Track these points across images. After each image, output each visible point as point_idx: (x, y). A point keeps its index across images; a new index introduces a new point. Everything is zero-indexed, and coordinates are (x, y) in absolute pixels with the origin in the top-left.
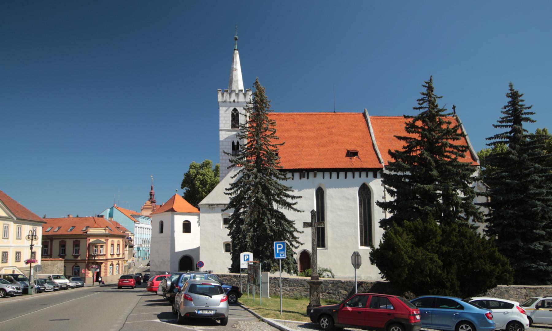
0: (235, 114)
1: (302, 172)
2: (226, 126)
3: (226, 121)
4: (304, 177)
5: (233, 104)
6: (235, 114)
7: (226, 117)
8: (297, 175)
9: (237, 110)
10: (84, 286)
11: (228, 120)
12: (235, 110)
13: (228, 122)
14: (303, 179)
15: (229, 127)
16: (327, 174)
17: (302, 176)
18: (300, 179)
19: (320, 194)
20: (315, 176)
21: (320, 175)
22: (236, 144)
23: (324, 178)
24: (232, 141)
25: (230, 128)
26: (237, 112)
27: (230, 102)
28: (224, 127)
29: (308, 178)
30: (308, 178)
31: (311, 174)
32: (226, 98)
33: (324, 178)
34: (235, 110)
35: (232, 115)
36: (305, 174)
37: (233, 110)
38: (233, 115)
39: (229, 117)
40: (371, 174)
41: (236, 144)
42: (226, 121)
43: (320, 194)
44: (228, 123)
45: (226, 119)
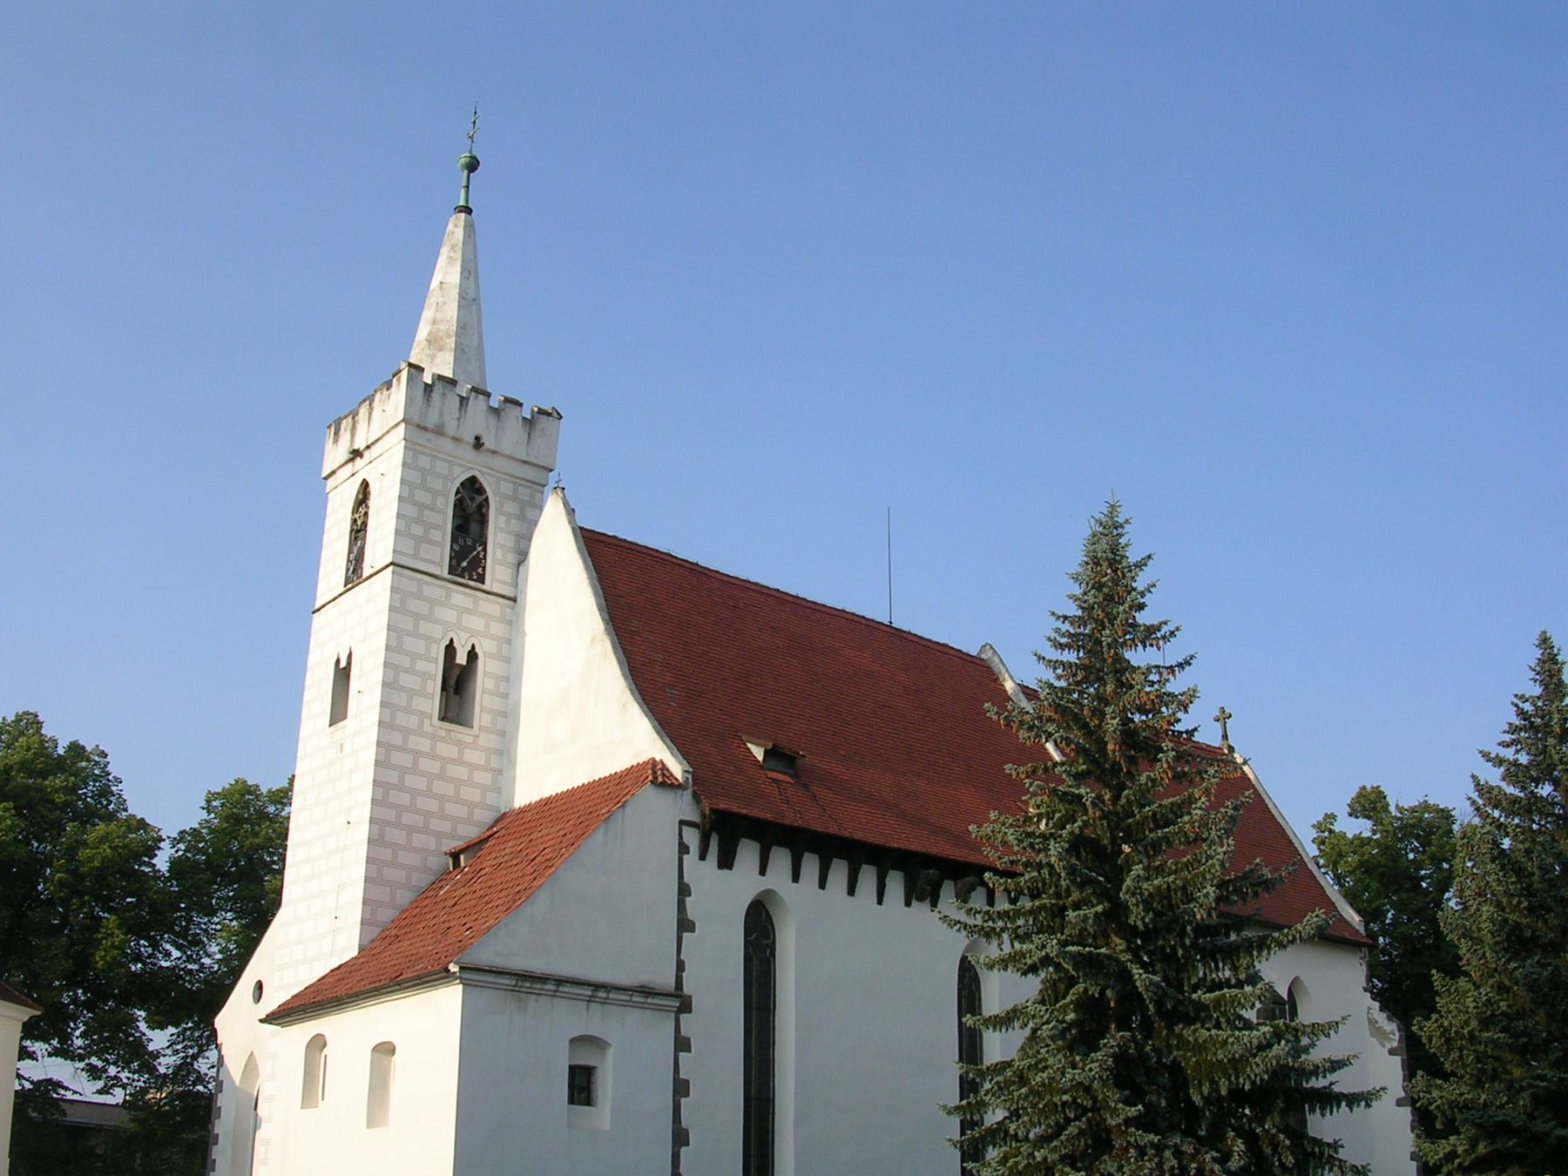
0: (472, 507)
3: (428, 526)
5: (469, 454)
11: (438, 527)
12: (472, 487)
13: (436, 535)
22: (461, 659)
25: (445, 574)
26: (480, 499)
27: (456, 439)
28: (416, 556)
32: (441, 414)
34: (472, 487)
38: (459, 505)
41: (461, 659)
42: (428, 526)
44: (432, 543)
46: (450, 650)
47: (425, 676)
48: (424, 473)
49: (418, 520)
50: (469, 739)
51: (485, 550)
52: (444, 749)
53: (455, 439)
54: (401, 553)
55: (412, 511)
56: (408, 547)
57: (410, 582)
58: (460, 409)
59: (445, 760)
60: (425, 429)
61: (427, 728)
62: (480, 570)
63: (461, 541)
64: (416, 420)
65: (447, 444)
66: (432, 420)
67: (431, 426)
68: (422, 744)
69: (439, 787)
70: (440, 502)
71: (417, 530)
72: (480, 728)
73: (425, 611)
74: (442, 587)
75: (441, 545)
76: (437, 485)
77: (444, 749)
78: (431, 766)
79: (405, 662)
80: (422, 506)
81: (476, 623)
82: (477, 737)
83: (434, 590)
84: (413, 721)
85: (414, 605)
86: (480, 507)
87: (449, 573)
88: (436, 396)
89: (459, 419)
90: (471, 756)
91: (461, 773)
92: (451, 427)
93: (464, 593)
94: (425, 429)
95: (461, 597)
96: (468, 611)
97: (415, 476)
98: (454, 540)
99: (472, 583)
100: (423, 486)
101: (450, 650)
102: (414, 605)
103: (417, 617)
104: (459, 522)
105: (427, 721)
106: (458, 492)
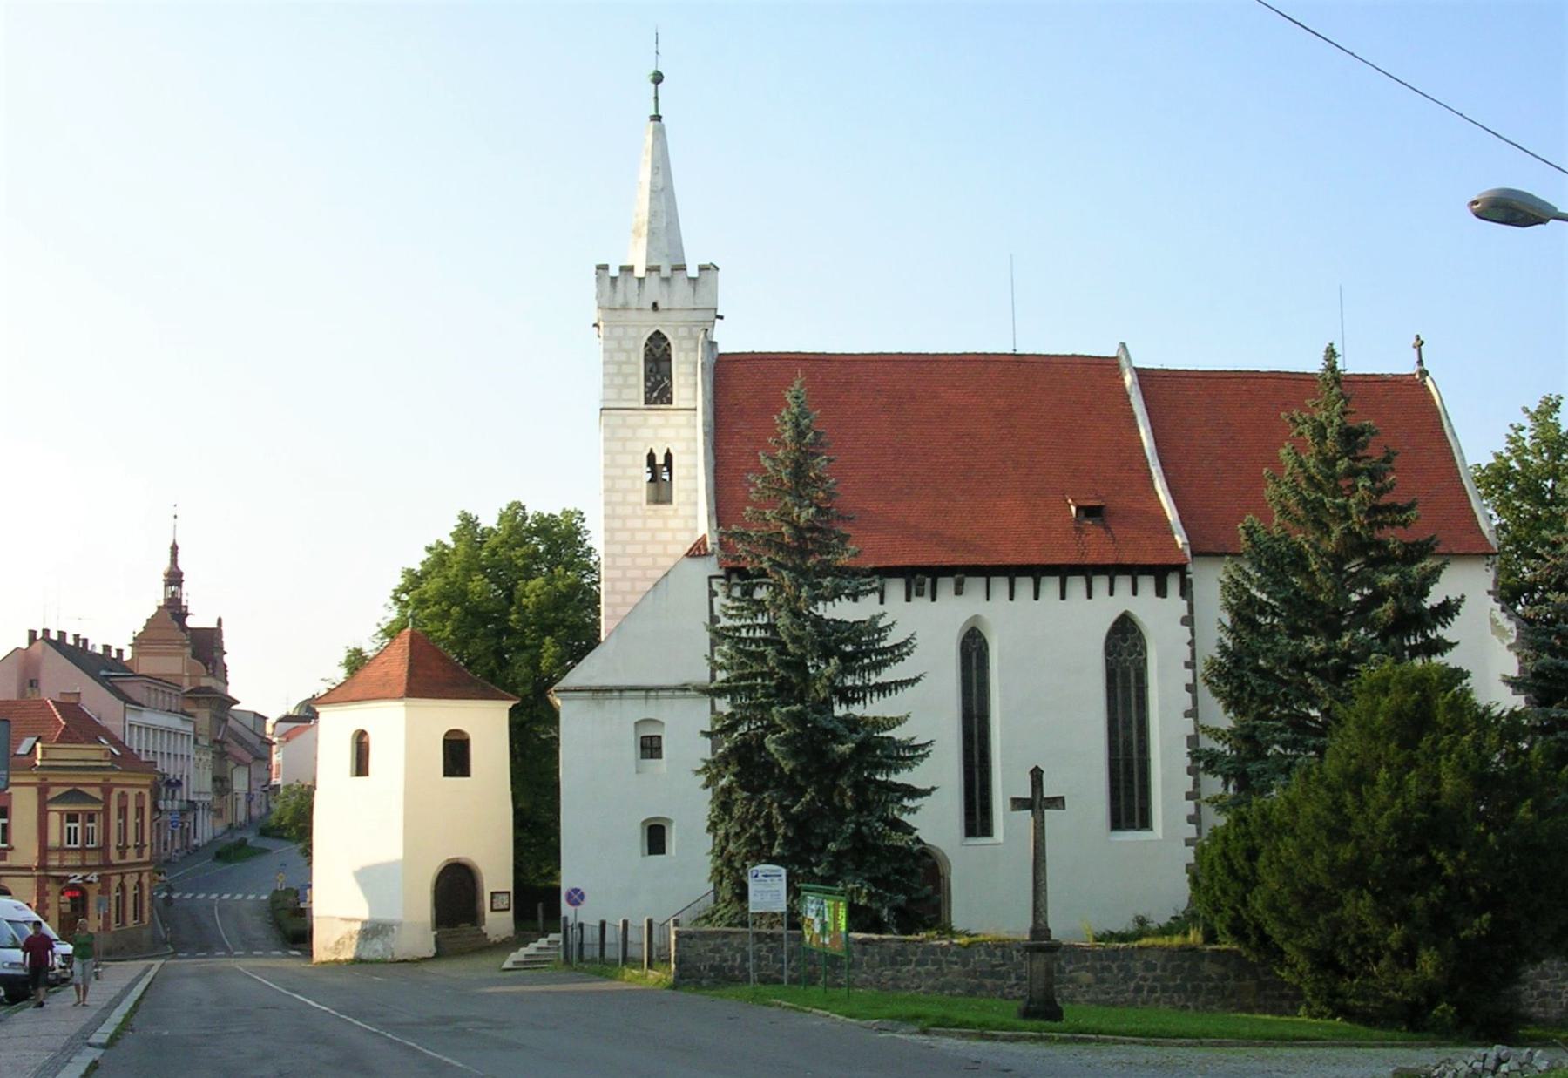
0: (658, 352)
1: (914, 576)
2: (624, 397)
3: (626, 376)
4: (920, 594)
6: (658, 352)
7: (628, 362)
8: (896, 588)
9: (665, 339)
10: (639, 941)
13: (632, 380)
14: (916, 600)
15: (638, 400)
16: (1000, 585)
17: (913, 590)
18: (908, 600)
19: (974, 654)
20: (959, 592)
21: (975, 585)
22: (660, 460)
23: (988, 599)
24: (648, 452)
25: (642, 405)
28: (620, 399)
29: (934, 599)
30: (934, 599)
31: (946, 585)
32: (625, 295)
33: (988, 599)
35: (646, 355)
36: (923, 584)
37: (650, 339)
39: (636, 364)
40: (1147, 584)
41: (660, 460)
43: (974, 654)
44: (630, 386)
45: (627, 369)
46: (651, 457)
47: (634, 478)
48: (619, 340)
49: (619, 374)
50: (671, 513)
51: (671, 380)
52: (652, 523)
53: (637, 309)
54: (608, 400)
55: (613, 369)
56: (612, 393)
57: (615, 418)
58: (639, 287)
59: (654, 531)
60: (615, 309)
61: (639, 512)
62: (669, 395)
63: (653, 379)
64: (607, 305)
65: (633, 315)
66: (619, 300)
67: (618, 306)
68: (638, 523)
69: (651, 549)
70: (633, 358)
71: (619, 381)
72: (678, 504)
73: (630, 435)
74: (640, 415)
75: (637, 386)
76: (628, 344)
77: (658, 524)
78: (647, 536)
79: (619, 472)
80: (620, 364)
81: (669, 433)
82: (676, 510)
83: (634, 418)
84: (628, 510)
85: (622, 433)
86: (665, 350)
87: (646, 404)
88: (620, 284)
89: (639, 295)
90: (673, 524)
91: (667, 536)
92: (634, 303)
93: (658, 415)
94: (615, 309)
95: (656, 417)
96: (661, 426)
97: (613, 344)
98: (647, 379)
99: (663, 406)
100: (621, 349)
101: (651, 457)
102: (622, 433)
103: (624, 440)
104: (650, 365)
105: (638, 508)
106: (646, 345)
